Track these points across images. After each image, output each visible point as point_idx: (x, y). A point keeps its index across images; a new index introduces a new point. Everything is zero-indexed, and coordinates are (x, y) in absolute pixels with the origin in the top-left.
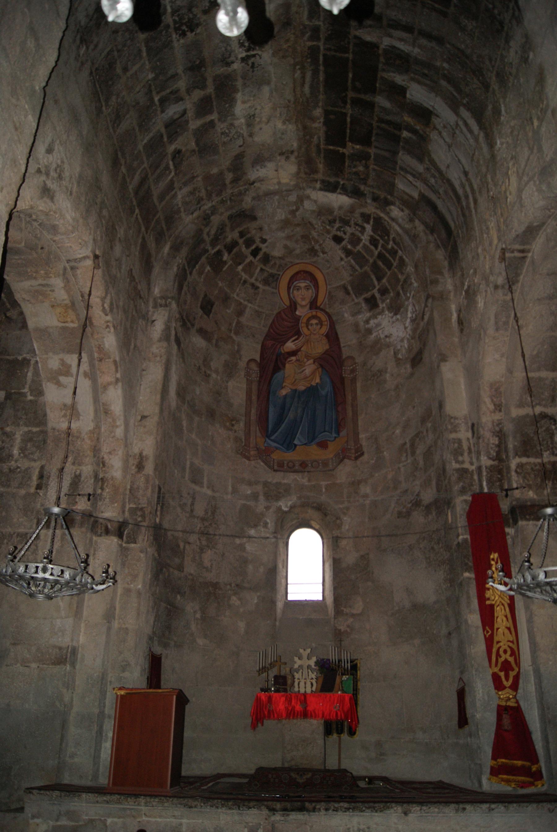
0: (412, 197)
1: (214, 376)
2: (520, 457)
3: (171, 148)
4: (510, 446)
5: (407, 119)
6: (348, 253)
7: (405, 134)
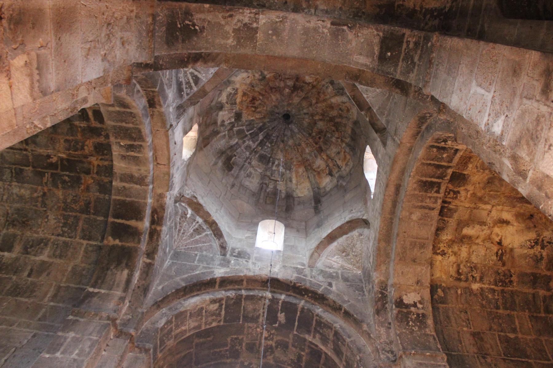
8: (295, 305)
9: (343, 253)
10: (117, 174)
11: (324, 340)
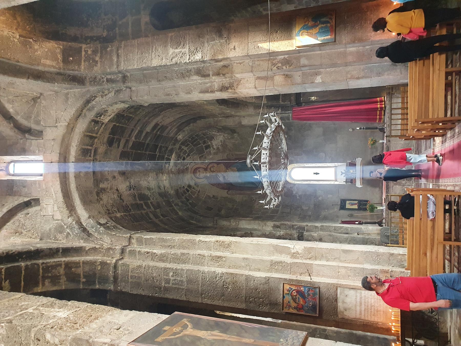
0: (177, 130)
1: (235, 206)
2: (280, 100)
4: (276, 103)
6: (188, 155)
7: (158, 133)
8: (18, 266)
9: (16, 234)
11: (55, 280)
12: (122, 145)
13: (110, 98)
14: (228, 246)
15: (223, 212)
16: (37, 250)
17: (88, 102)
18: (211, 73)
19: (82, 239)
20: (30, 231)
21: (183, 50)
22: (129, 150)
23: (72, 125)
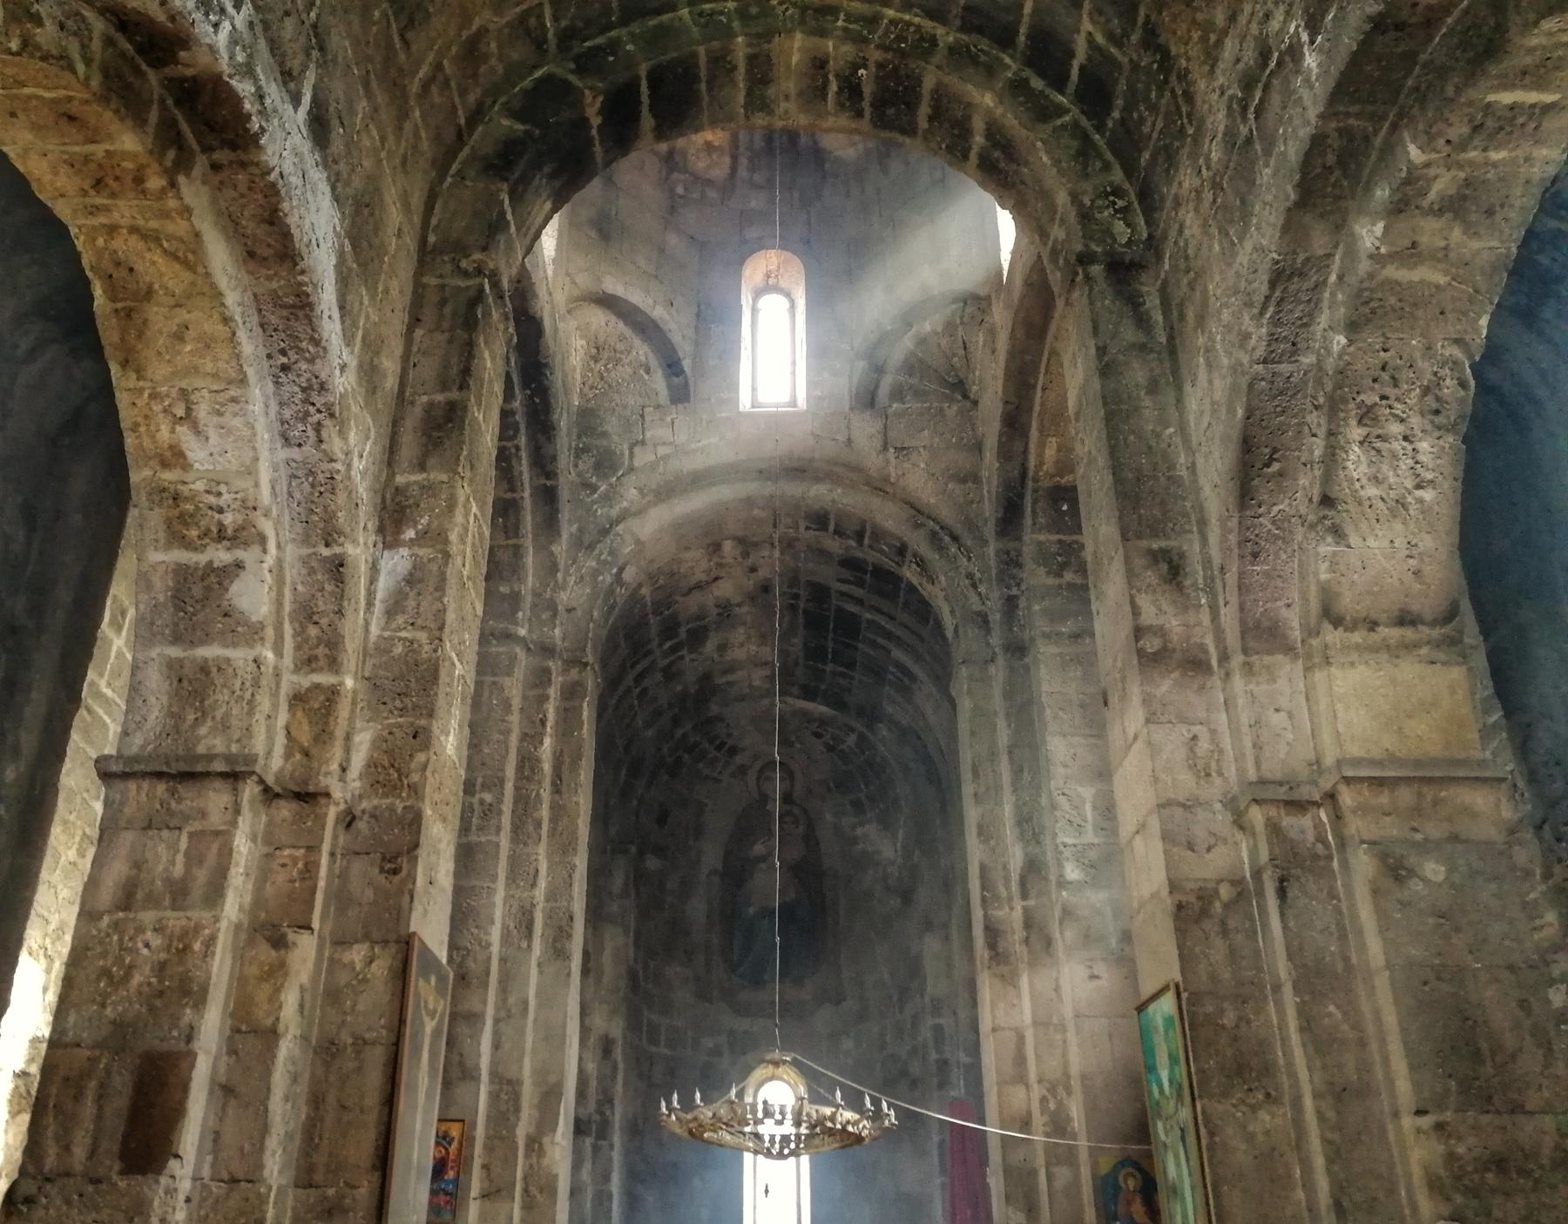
3: (638, 690)
5: (892, 669)
6: (831, 749)
7: (890, 676)
9: (598, 348)
10: (766, 46)
12: (845, 588)
13: (967, 598)
14: (558, 951)
15: (652, 863)
16: (554, 429)
17: (955, 538)
18: (1031, 903)
19: (580, 529)
20: (602, 378)
21: (1089, 827)
22: (834, 602)
23: (891, 490)
